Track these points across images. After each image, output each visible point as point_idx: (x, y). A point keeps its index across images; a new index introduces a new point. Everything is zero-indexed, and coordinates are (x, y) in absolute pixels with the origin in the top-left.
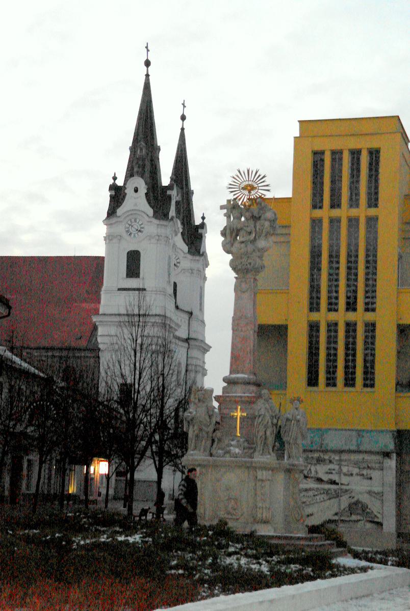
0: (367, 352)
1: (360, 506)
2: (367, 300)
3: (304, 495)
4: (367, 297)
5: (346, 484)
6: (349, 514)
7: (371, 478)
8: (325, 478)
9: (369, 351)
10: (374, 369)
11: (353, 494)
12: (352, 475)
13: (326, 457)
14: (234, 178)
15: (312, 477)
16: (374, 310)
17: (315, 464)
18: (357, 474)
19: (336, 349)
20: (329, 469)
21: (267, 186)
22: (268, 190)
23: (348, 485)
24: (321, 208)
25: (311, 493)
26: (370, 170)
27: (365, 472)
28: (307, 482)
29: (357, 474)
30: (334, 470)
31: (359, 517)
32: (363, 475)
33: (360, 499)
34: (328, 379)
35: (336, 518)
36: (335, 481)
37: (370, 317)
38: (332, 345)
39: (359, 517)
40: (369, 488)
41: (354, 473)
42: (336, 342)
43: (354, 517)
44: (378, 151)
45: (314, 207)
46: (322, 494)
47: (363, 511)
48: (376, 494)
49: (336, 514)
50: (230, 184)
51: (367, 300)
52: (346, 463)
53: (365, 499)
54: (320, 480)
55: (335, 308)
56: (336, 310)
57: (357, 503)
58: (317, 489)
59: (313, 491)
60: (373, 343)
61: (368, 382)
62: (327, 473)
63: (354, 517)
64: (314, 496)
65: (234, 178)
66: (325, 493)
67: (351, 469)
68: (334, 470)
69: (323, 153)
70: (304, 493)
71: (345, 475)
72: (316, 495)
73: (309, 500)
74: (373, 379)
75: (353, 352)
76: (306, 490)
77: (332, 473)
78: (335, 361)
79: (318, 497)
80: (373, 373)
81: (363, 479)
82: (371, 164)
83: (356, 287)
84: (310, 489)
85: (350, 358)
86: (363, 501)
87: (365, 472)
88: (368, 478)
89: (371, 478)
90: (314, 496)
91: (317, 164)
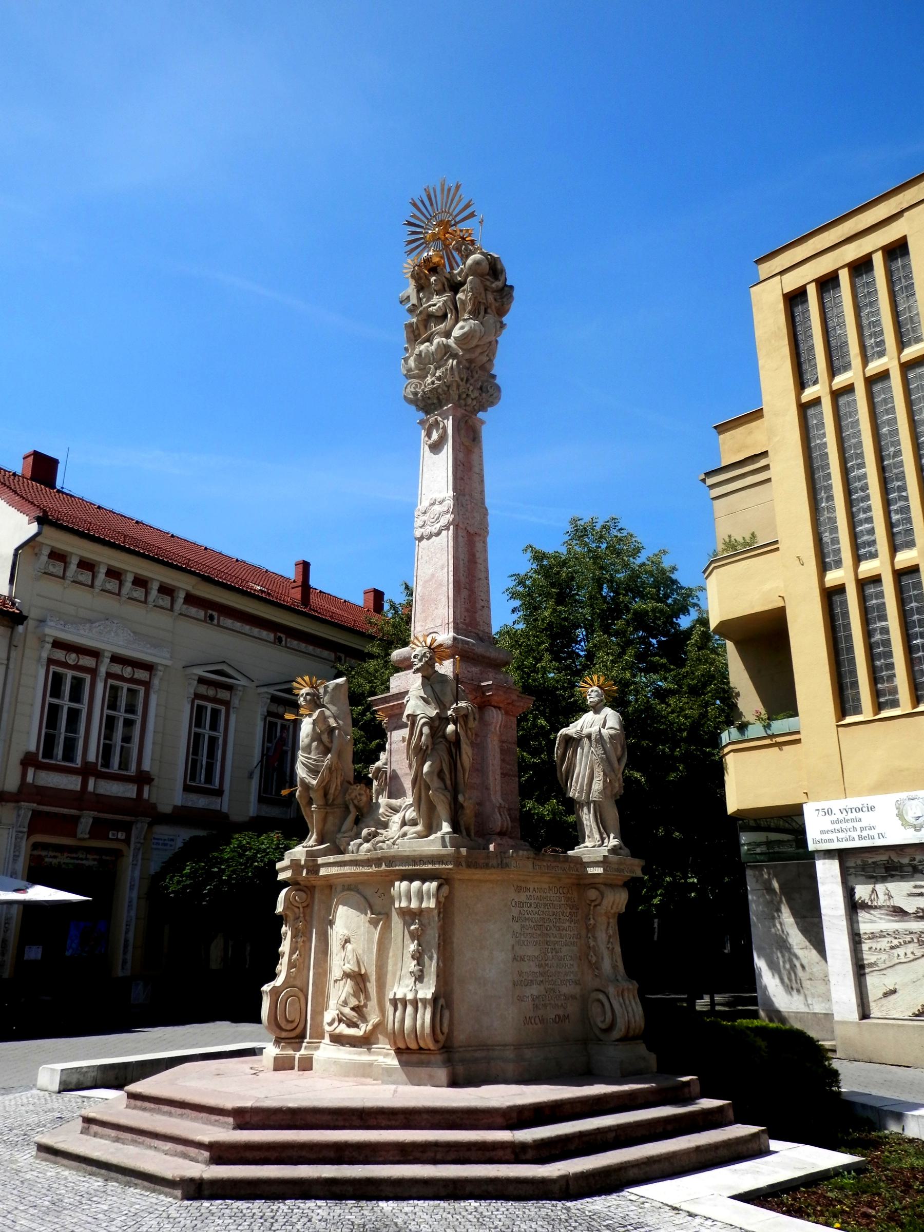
13: (905, 861)
15: (880, 907)
25: (884, 943)
28: (873, 918)
46: (909, 942)
54: (899, 912)
58: (896, 932)
59: (890, 939)
62: (910, 895)
64: (892, 948)
66: (916, 940)
72: (898, 947)
73: (884, 956)
79: (901, 951)
84: (882, 935)
90: (892, 948)
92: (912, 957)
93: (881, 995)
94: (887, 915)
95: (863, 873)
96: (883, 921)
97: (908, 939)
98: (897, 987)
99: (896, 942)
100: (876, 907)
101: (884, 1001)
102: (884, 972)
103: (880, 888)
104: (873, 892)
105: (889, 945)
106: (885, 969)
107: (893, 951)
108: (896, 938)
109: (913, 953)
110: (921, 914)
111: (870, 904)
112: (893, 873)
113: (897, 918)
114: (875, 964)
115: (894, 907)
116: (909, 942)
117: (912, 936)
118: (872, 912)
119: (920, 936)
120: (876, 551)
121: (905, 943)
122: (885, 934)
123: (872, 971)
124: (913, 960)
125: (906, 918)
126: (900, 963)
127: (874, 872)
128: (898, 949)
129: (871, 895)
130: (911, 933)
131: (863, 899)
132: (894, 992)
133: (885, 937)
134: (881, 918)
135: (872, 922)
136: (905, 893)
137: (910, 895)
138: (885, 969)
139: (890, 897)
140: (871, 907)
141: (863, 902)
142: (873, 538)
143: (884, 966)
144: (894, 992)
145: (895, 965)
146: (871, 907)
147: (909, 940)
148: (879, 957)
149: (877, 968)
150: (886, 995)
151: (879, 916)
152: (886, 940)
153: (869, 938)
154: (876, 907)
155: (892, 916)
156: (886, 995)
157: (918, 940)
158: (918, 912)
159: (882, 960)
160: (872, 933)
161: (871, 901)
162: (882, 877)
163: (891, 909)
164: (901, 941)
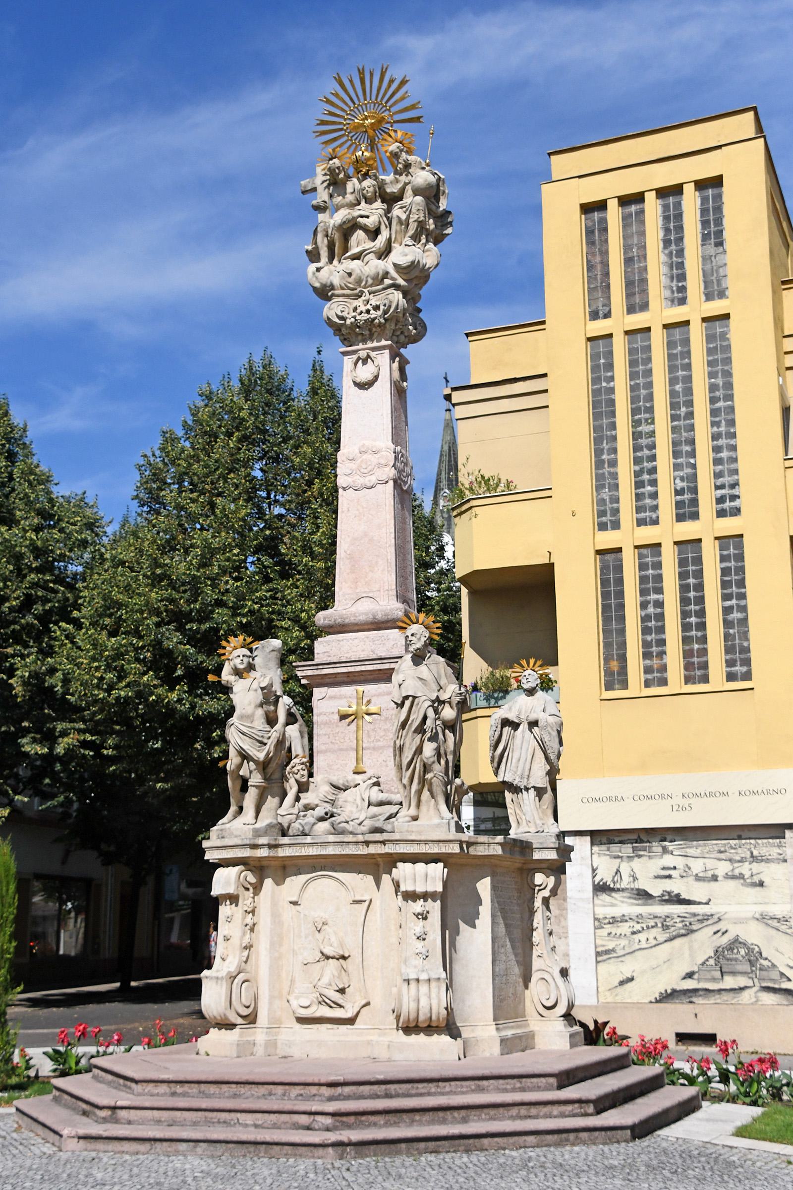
0: (728, 603)
1: (742, 952)
2: (720, 492)
3: (609, 934)
4: (717, 488)
5: (704, 901)
6: (718, 974)
7: (761, 884)
8: (656, 889)
9: (734, 602)
10: (748, 640)
11: (722, 926)
12: (715, 878)
14: (328, 101)
15: (623, 890)
16: (736, 512)
17: (630, 858)
18: (728, 877)
19: (660, 604)
20: (664, 868)
21: (413, 107)
22: (418, 119)
23: (707, 904)
24: (607, 315)
25: (625, 928)
26: (705, 223)
27: (745, 869)
29: (728, 877)
30: (675, 868)
31: (742, 981)
32: (741, 876)
33: (743, 937)
34: (648, 670)
35: (690, 984)
36: (678, 895)
37: (729, 526)
38: (653, 597)
39: (742, 981)
40: (759, 909)
41: (720, 873)
42: (660, 591)
43: (729, 982)
44: (717, 182)
45: (594, 316)
46: (653, 927)
47: (752, 963)
48: (779, 920)
49: (690, 975)
50: (323, 123)
51: (720, 492)
52: (699, 851)
53: (753, 935)
54: (643, 895)
55: (651, 518)
56: (655, 522)
57: (736, 942)
58: (640, 916)
59: (631, 923)
60: (741, 583)
61: (739, 669)
62: (657, 877)
63: (729, 982)
64: (634, 933)
65: (328, 101)
66: (659, 925)
67: (710, 863)
68: (675, 868)
69: (602, 206)
70: (608, 928)
71: (698, 878)
72: (640, 932)
73: (623, 942)
74: (747, 662)
75: (697, 608)
76: (614, 921)
77: (669, 877)
78: (661, 630)
79: (642, 937)
80: (747, 650)
81: (742, 884)
82: (704, 211)
83: (694, 466)
84: (623, 919)
85: (693, 620)
86: (750, 941)
87: (745, 869)
88: (754, 885)
89: (761, 884)
90: (634, 933)
91: (593, 232)
92: (654, 942)
93: (616, 983)
94: (630, 898)
95: (608, 853)
96: (625, 905)
97: (652, 923)
98: (635, 974)
99: (638, 927)
100: (618, 890)
101: (619, 989)
102: (620, 959)
103: (625, 868)
104: (616, 873)
105: (631, 930)
106: (624, 955)
107: (635, 936)
108: (638, 923)
109: (655, 938)
110: (667, 897)
111: (612, 886)
112: (641, 853)
113: (640, 902)
114: (613, 950)
115: (638, 890)
116: (653, 927)
117: (656, 920)
118: (613, 894)
119: (665, 921)
120: (658, 517)
121: (648, 927)
122: (627, 918)
123: (610, 958)
124: (655, 946)
125: (650, 902)
126: (640, 949)
127: (620, 851)
128: (640, 935)
129: (614, 877)
130: (655, 917)
131: (604, 881)
132: (632, 979)
133: (626, 921)
134: (623, 902)
135: (613, 905)
136: (652, 875)
137: (657, 877)
138: (624, 955)
139: (635, 879)
140: (613, 890)
141: (605, 884)
142: (655, 503)
143: (621, 953)
144: (632, 979)
145: (634, 951)
146: (613, 890)
147: (653, 924)
148: (618, 943)
149: (615, 955)
150: (622, 983)
151: (622, 899)
152: (627, 925)
153: (609, 923)
154: (618, 890)
155: (635, 899)
156: (622, 983)
157: (663, 925)
158: (663, 895)
159: (622, 946)
160: (613, 918)
161: (614, 883)
162: (628, 857)
163: (635, 892)
164: (644, 926)
